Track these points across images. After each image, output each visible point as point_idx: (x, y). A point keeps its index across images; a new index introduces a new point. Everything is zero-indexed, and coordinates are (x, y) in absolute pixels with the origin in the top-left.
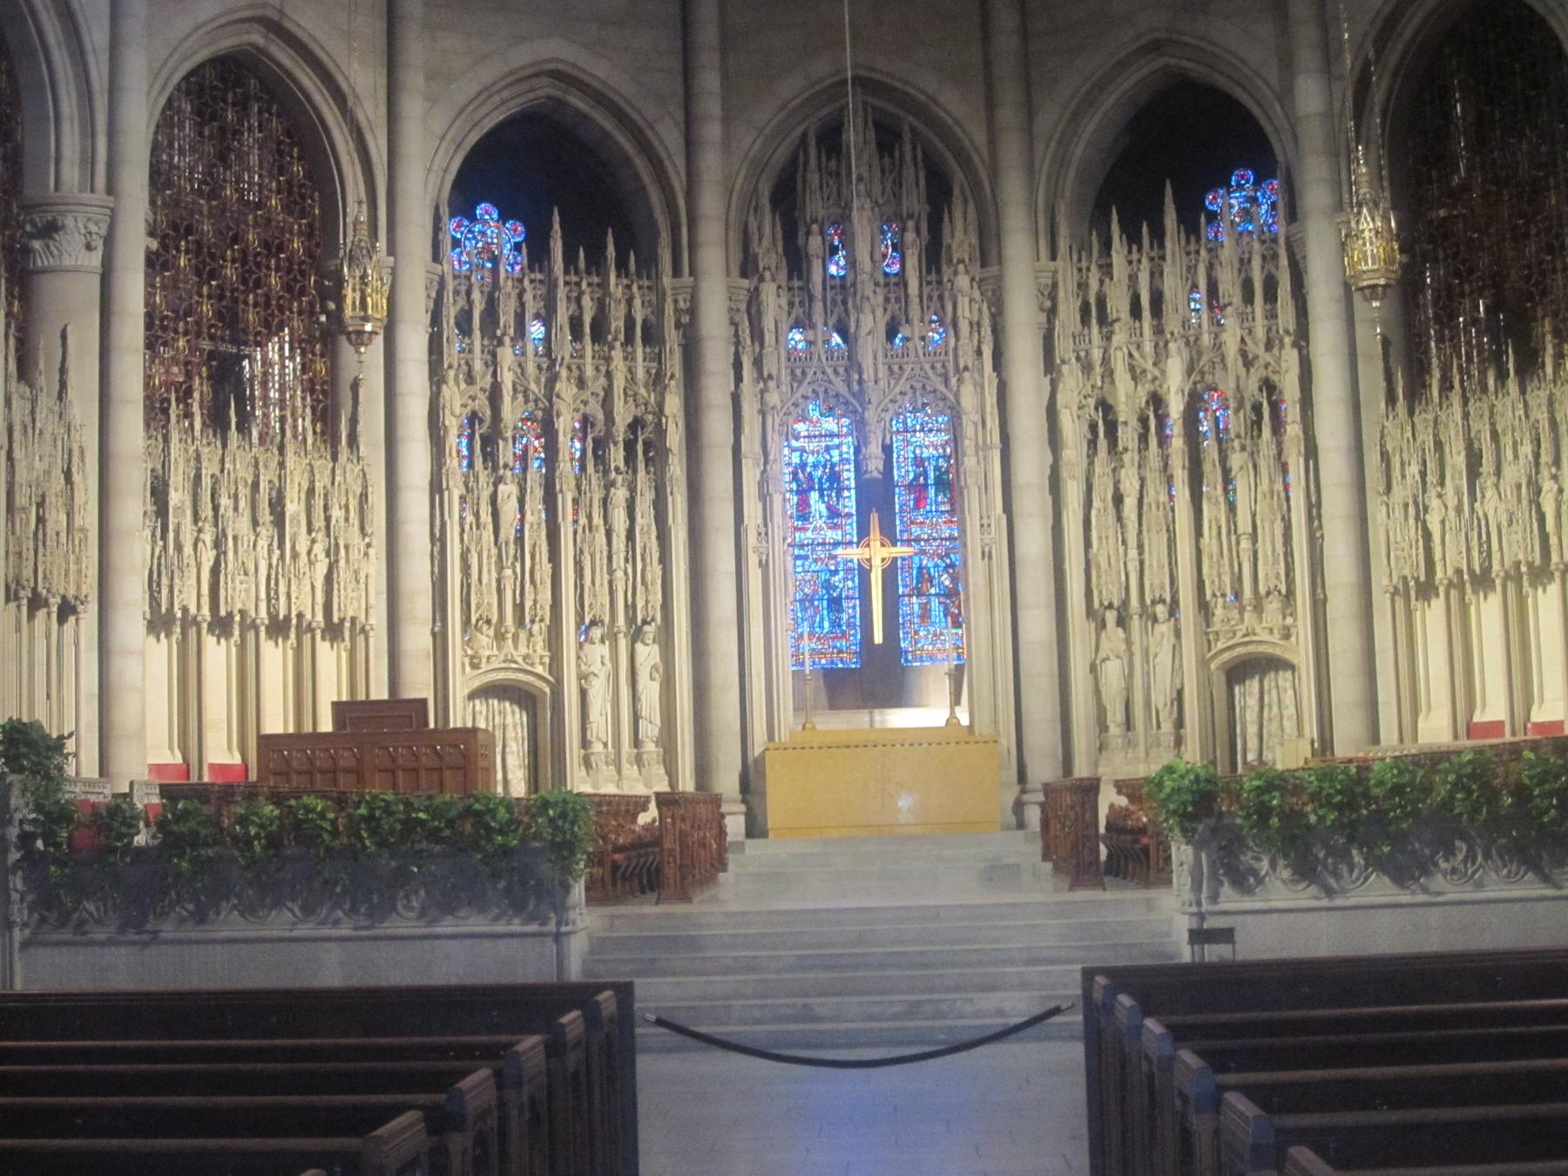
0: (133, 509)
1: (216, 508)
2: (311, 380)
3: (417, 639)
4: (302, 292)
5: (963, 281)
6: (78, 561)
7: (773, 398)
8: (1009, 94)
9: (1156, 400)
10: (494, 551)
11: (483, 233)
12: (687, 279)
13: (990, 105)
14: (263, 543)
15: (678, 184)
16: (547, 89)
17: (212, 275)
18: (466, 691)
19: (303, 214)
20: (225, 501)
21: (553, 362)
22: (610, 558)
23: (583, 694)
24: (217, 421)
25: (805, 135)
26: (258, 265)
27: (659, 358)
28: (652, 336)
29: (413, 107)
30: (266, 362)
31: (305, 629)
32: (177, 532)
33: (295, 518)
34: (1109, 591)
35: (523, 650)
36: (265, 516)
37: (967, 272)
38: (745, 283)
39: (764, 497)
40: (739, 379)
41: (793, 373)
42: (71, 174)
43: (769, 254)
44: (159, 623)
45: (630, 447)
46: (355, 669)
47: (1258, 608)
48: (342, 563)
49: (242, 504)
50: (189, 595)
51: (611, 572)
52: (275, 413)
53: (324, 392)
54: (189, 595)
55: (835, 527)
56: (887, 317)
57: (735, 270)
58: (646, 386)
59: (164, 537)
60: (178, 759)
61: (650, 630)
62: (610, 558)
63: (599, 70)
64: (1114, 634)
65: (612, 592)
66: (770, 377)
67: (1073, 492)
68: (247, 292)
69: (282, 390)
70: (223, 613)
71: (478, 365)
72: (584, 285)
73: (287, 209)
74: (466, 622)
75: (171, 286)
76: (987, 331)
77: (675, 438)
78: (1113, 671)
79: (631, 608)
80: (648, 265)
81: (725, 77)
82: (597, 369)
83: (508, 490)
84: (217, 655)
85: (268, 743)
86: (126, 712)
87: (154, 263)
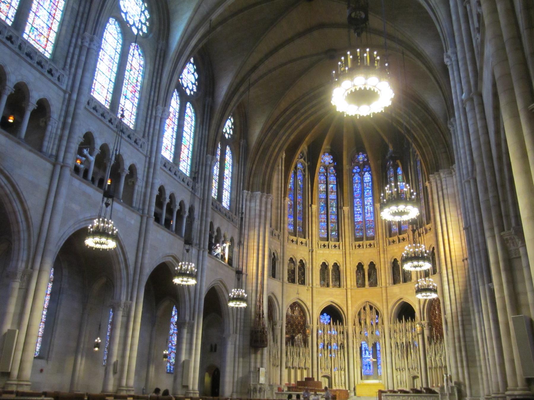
5: (380, 327)
7: (358, 341)
8: (385, 304)
9: (403, 343)
24: (293, 345)
27: (344, 336)
28: (343, 333)
29: (314, 307)
31: (302, 368)
34: (398, 367)
38: (354, 327)
39: (356, 353)
42: (278, 318)
44: (286, 367)
45: (340, 346)
47: (415, 369)
50: (290, 365)
54: (290, 365)
60: (288, 383)
61: (343, 370)
63: (336, 301)
64: (399, 372)
67: (393, 354)
71: (322, 337)
74: (321, 368)
75: (288, 329)
77: (346, 346)
78: (399, 377)
79: (340, 367)
80: (342, 324)
81: (351, 301)
83: (326, 352)
84: (293, 371)
85: (298, 382)
86: (283, 378)
87: (286, 327)
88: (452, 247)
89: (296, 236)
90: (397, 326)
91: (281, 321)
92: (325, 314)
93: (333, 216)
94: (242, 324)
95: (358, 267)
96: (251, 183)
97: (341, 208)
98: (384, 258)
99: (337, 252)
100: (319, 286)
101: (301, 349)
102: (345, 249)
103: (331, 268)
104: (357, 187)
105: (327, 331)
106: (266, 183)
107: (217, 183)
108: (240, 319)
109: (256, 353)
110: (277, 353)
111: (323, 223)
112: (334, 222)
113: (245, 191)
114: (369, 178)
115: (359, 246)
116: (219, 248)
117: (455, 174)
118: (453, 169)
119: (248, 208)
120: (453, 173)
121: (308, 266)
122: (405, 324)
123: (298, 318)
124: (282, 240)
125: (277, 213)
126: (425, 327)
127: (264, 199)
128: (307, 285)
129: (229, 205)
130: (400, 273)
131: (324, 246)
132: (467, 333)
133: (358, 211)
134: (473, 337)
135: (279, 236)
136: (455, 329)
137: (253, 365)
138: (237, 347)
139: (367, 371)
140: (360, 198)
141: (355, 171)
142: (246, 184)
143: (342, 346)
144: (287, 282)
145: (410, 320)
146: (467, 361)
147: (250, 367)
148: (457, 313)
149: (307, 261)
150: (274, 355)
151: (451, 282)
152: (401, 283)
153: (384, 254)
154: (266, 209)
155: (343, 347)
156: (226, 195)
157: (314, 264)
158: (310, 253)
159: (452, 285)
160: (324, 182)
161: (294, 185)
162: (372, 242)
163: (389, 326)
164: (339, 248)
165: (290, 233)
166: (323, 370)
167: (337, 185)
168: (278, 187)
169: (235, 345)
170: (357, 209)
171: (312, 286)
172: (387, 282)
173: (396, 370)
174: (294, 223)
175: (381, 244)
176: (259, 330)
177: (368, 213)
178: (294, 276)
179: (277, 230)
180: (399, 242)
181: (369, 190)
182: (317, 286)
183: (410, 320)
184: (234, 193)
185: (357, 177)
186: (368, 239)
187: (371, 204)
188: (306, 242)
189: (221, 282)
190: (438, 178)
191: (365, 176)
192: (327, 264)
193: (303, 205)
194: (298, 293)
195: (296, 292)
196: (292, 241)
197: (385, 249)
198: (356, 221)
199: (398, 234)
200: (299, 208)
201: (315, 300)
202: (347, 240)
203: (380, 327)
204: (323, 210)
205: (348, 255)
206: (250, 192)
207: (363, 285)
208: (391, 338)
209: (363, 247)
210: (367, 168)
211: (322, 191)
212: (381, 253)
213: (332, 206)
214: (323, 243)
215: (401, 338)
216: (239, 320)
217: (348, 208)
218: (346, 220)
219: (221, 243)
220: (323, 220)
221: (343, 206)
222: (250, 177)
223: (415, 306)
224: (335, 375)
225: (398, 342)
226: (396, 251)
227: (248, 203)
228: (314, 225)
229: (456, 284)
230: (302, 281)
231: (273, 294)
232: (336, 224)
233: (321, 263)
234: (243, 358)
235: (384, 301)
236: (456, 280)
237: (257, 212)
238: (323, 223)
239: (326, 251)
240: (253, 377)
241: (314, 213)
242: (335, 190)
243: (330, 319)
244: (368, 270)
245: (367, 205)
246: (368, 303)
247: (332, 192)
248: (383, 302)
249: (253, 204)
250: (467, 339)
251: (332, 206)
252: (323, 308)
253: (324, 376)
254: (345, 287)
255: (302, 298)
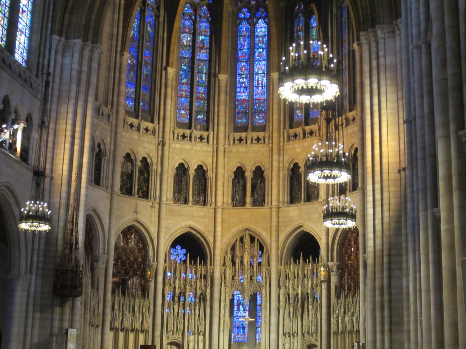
0: (109, 310)
1: (123, 309)
2: (141, 285)
3: (158, 333)
4: (140, 268)
5: (264, 269)
6: (99, 319)
7: (227, 290)
8: (274, 233)
9: (297, 295)
10: (173, 317)
11: (178, 252)
12: (212, 267)
13: (271, 236)
14: (131, 315)
15: (212, 248)
16: (187, 230)
17: (124, 266)
18: (166, 343)
19: (141, 253)
20: (124, 308)
21: (186, 282)
22: (195, 319)
23: (188, 345)
24: (124, 294)
25: (237, 239)
26: (133, 264)
27: (206, 282)
28: (205, 277)
29: (162, 235)
30: (133, 282)
31: (137, 331)
32: (116, 313)
33: (137, 311)
34: (287, 330)
35: (177, 336)
36: (131, 310)
37: (265, 267)
38: (224, 268)
39: (225, 309)
40: (221, 286)
41: (232, 285)
42: (101, 251)
43: (229, 262)
44: (112, 329)
45: (200, 298)
46: (146, 339)
47: (312, 335)
48: (145, 319)
49: (127, 308)
51: (195, 322)
52: (134, 290)
53: (144, 287)
54: (117, 324)
55: (245, 313)
56: (250, 275)
57: (222, 265)
58: (204, 287)
59: (113, 314)
61: (201, 333)
62: (195, 319)
63: (198, 227)
64: (288, 339)
65: (195, 326)
66: (227, 286)
68: (130, 269)
69: (136, 286)
70: (123, 328)
71: (172, 283)
72: (193, 267)
73: (138, 253)
76: (268, 279)
77: (208, 297)
79: (198, 329)
80: (205, 263)
81: (222, 228)
82: (194, 284)
83: (176, 306)
84: (121, 335)
88: (384, 149)
89: (137, 118)
90: (290, 268)
91: (106, 255)
92: (178, 247)
93: (201, 88)
94: (41, 259)
95: (235, 173)
96: (66, 22)
97: (216, 76)
98: (279, 162)
99: (204, 148)
100: (172, 202)
101: (137, 301)
102: (217, 144)
103: (192, 172)
104: (244, 43)
105: (180, 273)
106: (92, 24)
107: (6, 20)
108: (38, 250)
109: (62, 305)
110: (97, 306)
111: (183, 100)
112: (202, 99)
113: (55, 37)
114: (263, 30)
115: (240, 140)
116: (6, 131)
117: (400, 35)
118: (397, 25)
119: (59, 65)
120: (397, 32)
121: (155, 168)
122: (303, 267)
123: (133, 252)
124: (114, 122)
125: (109, 78)
126: (332, 271)
127: (87, 53)
128: (152, 199)
129: (25, 58)
130: (301, 187)
131: (184, 136)
132: (394, 284)
133: (243, 83)
134: (401, 288)
135: (109, 116)
136: (378, 275)
137: (56, 324)
138: (32, 294)
139: (239, 336)
140: (246, 62)
141: (243, 16)
142: (57, 26)
143: (203, 298)
144: (119, 193)
145: (311, 259)
146: (391, 323)
147: (52, 327)
148: (382, 251)
149: (154, 161)
150: (92, 309)
151: (378, 203)
152: (302, 202)
153: (279, 155)
154: (90, 68)
155: (203, 298)
156: (22, 41)
157: (166, 165)
158: (160, 147)
159: (378, 209)
160: (190, 30)
161: (139, 31)
162: (261, 135)
163: (277, 269)
164: (208, 142)
165: (128, 113)
166: (170, 334)
167: (211, 36)
168: (112, 34)
169: (28, 292)
170: (241, 80)
171: (160, 200)
172: (281, 200)
173: (284, 334)
174: (136, 95)
175: (275, 139)
176: (70, 269)
177: (258, 87)
178: (131, 184)
179: (106, 106)
180: (304, 136)
181: (263, 49)
182: (168, 202)
183: (311, 259)
184: (36, 38)
185: (244, 27)
186: (255, 129)
187: (264, 73)
188: (154, 128)
189: (8, 187)
190: (372, 39)
191: (258, 26)
192: (186, 166)
193: (152, 66)
194: (136, 212)
195: (134, 209)
196: (132, 126)
197: (281, 148)
198: (238, 98)
199: (303, 125)
200: (145, 71)
201: (163, 224)
202: (222, 128)
203: (264, 269)
204: (186, 76)
205: (221, 154)
206: (63, 39)
207: (243, 203)
208: (279, 287)
209: (246, 142)
210: (262, 13)
211: (186, 46)
212: (275, 152)
213: (201, 72)
214: (181, 131)
215: (295, 287)
216: (36, 252)
217: (226, 76)
218: (222, 97)
219: (10, 122)
220: (184, 94)
221: (219, 72)
222: (65, 12)
223: (321, 239)
224: (188, 342)
225: (291, 294)
226: (298, 150)
227: (59, 57)
228: (169, 101)
229: (386, 207)
230: (143, 192)
231: (94, 211)
232: (206, 102)
233: (177, 165)
234: (41, 312)
235: (274, 229)
236: (386, 201)
237: (75, 74)
238: (183, 100)
239: (187, 145)
240: (56, 343)
241: (170, 82)
242: (207, 45)
243: (186, 255)
244: (252, 179)
245: (257, 74)
246: (247, 232)
247: (202, 48)
248: (271, 231)
249: (67, 60)
250: (394, 291)
251: (201, 72)
252: (176, 237)
253: (172, 343)
254: (213, 205)
255: (143, 220)
